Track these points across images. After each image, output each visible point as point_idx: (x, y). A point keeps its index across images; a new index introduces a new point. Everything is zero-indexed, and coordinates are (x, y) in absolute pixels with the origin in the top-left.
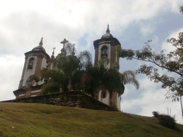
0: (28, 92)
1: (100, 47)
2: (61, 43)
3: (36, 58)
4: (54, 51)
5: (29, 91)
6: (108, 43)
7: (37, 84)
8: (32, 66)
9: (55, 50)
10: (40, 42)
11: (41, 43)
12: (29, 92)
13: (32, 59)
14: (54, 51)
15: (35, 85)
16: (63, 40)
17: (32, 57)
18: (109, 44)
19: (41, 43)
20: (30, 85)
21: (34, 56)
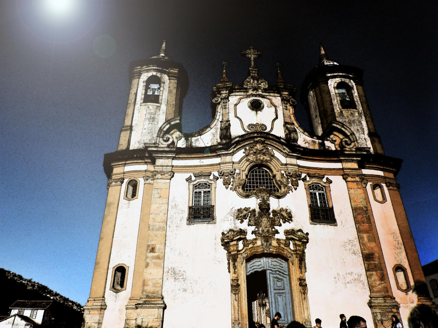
1: (332, 83)
3: (165, 78)
5: (168, 158)
8: (158, 96)
15: (182, 144)
17: (154, 73)
18: (352, 81)
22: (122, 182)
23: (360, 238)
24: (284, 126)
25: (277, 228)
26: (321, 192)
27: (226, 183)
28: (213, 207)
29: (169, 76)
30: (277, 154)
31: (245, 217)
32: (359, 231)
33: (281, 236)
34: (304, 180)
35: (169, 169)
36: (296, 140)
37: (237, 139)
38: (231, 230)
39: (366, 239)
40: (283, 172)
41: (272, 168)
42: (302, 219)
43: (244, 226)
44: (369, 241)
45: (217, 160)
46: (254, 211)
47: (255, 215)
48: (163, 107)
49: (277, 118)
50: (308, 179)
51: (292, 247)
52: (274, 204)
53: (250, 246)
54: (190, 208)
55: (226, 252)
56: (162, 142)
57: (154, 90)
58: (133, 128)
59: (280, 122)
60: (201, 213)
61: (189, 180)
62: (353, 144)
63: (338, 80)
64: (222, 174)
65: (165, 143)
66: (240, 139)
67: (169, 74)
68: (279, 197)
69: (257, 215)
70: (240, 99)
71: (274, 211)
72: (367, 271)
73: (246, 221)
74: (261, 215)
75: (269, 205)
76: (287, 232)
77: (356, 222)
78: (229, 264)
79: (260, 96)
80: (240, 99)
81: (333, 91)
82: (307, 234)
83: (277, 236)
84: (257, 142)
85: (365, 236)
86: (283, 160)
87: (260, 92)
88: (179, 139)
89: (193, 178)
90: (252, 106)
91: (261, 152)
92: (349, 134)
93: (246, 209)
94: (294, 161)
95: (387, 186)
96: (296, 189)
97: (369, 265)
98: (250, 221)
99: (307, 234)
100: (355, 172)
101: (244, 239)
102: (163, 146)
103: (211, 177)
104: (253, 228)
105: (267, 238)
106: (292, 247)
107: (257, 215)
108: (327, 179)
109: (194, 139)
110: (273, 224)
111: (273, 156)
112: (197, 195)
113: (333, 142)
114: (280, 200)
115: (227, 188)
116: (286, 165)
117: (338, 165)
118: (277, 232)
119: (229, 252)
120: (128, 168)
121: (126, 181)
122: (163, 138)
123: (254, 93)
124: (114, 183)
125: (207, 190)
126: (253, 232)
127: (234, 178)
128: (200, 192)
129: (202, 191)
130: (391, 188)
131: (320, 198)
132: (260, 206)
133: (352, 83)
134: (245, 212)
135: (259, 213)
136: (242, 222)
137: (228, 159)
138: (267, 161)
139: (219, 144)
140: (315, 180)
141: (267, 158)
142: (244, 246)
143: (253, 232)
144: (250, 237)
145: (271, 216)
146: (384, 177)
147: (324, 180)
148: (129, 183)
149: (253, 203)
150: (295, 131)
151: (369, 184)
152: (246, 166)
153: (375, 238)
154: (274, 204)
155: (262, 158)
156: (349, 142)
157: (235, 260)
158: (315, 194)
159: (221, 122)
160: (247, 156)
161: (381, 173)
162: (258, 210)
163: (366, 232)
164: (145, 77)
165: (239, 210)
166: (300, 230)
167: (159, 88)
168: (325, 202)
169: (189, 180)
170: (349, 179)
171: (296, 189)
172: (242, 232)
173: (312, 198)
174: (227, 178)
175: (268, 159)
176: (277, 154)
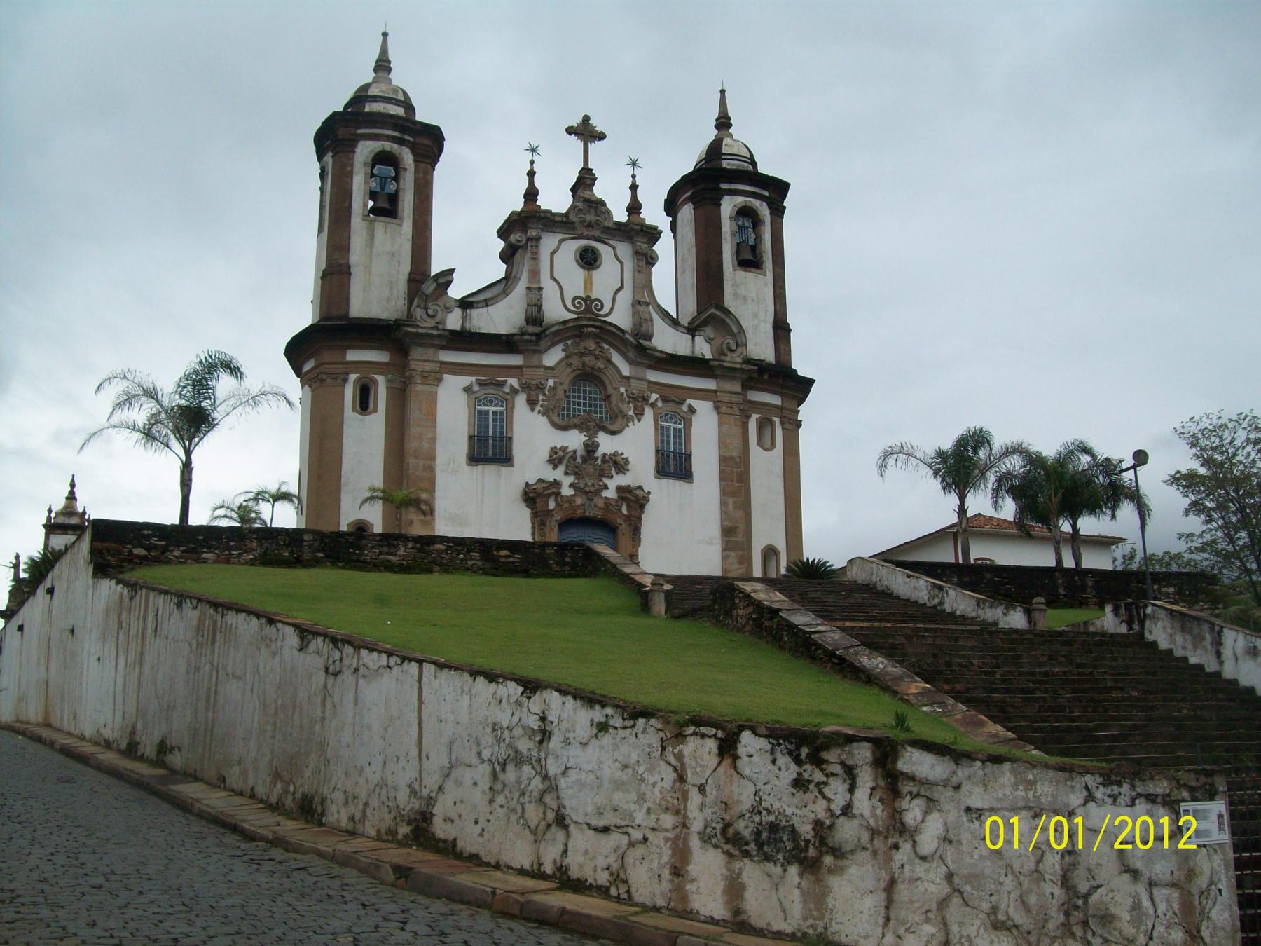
0: (420, 350)
1: (728, 206)
2: (570, 131)
3: (407, 158)
4: (532, 162)
6: (761, 198)
7: (464, 318)
8: (394, 199)
9: (536, 158)
10: (377, 56)
11: (383, 65)
12: (428, 353)
13: (383, 158)
14: (532, 162)
15: (454, 321)
16: (580, 120)
17: (388, 146)
18: (764, 204)
19: (383, 65)
20: (438, 319)
21: (395, 146)
22: (346, 380)
23: (723, 504)
24: (633, 305)
25: (606, 481)
26: (678, 426)
27: (532, 403)
28: (511, 438)
29: (414, 153)
30: (617, 359)
31: (560, 461)
32: (724, 493)
33: (610, 493)
34: (653, 405)
35: (436, 367)
36: (649, 337)
37: (556, 328)
38: (540, 480)
39: (731, 507)
40: (622, 389)
41: (607, 382)
42: (642, 471)
43: (558, 474)
44: (735, 508)
45: (515, 360)
46: (575, 452)
47: (575, 459)
48: (407, 227)
49: (622, 287)
50: (660, 404)
51: (624, 510)
52: (607, 445)
53: (566, 505)
54: (471, 438)
55: (528, 511)
56: (425, 317)
57: (383, 180)
58: (353, 270)
59: (625, 298)
60: (490, 449)
61: (468, 390)
62: (740, 350)
63: (740, 200)
64: (526, 387)
65: (429, 320)
66: (561, 327)
67: (414, 148)
68: (613, 433)
69: (579, 460)
70: (561, 242)
71: (604, 455)
72: (723, 550)
73: (561, 469)
74: (585, 460)
75: (598, 446)
76: (620, 489)
77: (721, 479)
78: (533, 528)
79: (595, 239)
80: (561, 242)
81: (727, 226)
82: (649, 493)
83: (605, 494)
84: (589, 335)
85: (730, 501)
86: (625, 369)
87: (597, 233)
88: (448, 310)
89: (476, 388)
90: (582, 258)
91: (591, 353)
92: (735, 330)
93: (564, 449)
94: (639, 372)
95: (782, 423)
96: (639, 420)
97: (727, 542)
98: (567, 467)
99: (649, 493)
100: (735, 399)
101: (558, 494)
102: (425, 325)
103: (507, 389)
104: (571, 479)
105: (592, 494)
106: (624, 510)
107: (579, 460)
108: (690, 406)
109: (475, 312)
110: (603, 474)
111: (609, 361)
112: (483, 415)
113: (709, 340)
114: (615, 438)
115: (533, 410)
116: (628, 378)
117: (710, 384)
118: (606, 487)
119: (535, 515)
120: (353, 356)
121: (353, 377)
122: (426, 309)
123: (586, 233)
124: (329, 380)
125: (498, 408)
126: (571, 485)
127: (544, 395)
128: (487, 413)
129: (492, 409)
130: (787, 426)
131: (674, 437)
132: (586, 445)
133: (764, 210)
134: (561, 454)
135: (582, 457)
136: (555, 468)
137: (534, 360)
138: (600, 370)
139: (523, 334)
140: (671, 406)
141: (600, 364)
142: (558, 504)
143: (571, 485)
144: (567, 491)
145: (599, 462)
146: (781, 408)
147: (685, 408)
148: (355, 382)
149: (574, 440)
150: (651, 320)
151: (755, 417)
152: (566, 376)
153: (746, 506)
154: (607, 445)
155: (592, 364)
156: (734, 347)
157: (543, 524)
158: (668, 429)
159: (528, 288)
160: (567, 357)
161: (775, 400)
162: (581, 452)
163: (733, 494)
164: (365, 150)
165: (554, 451)
166: (640, 488)
167: (396, 179)
168: (680, 444)
169: (468, 390)
170: (724, 409)
171: (639, 420)
172: (557, 484)
173: (662, 434)
174: (533, 392)
175: (602, 366)
176: (617, 359)
